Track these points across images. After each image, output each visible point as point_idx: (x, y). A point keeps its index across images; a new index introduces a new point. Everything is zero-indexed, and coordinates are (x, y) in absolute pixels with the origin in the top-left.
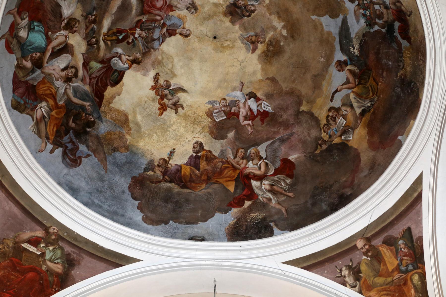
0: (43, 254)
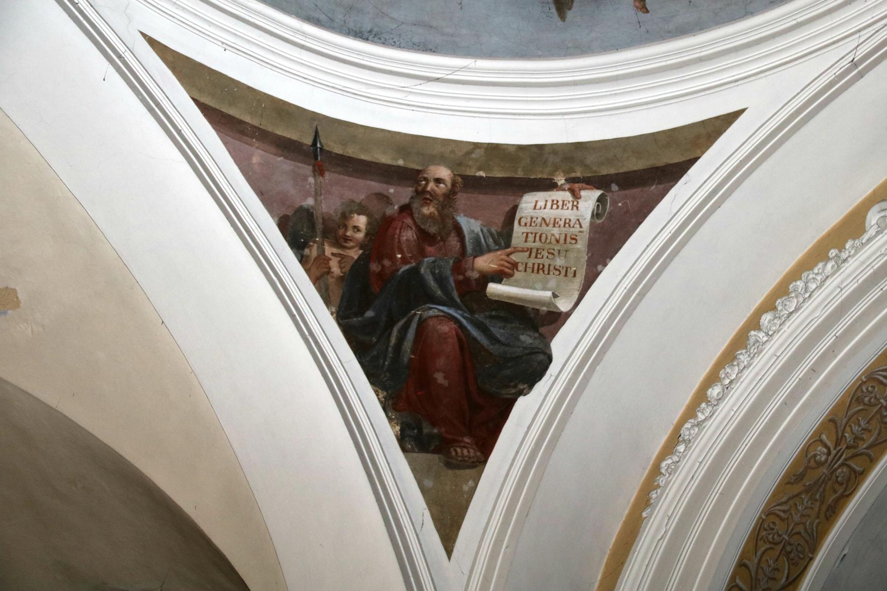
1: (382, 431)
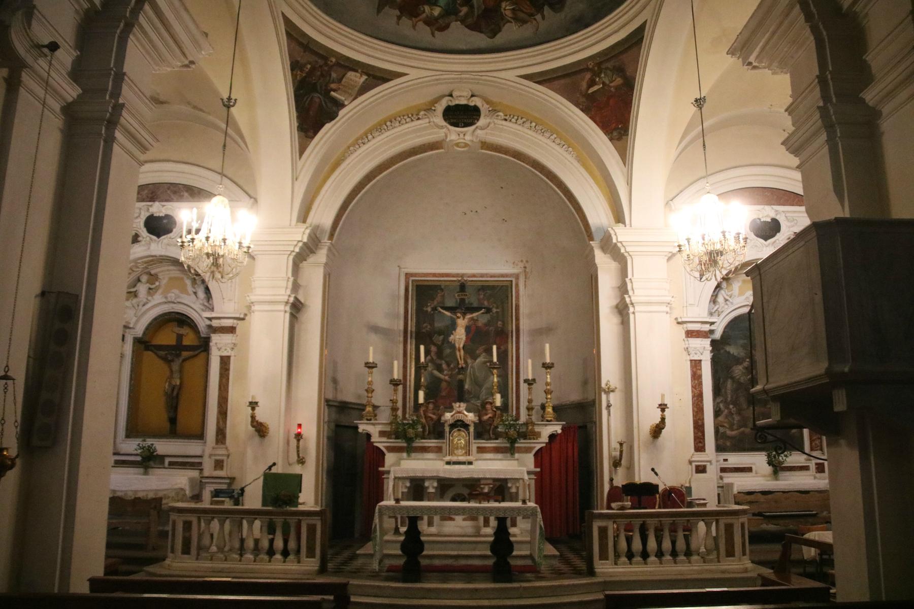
0: (604, 83)
1: (296, 124)
